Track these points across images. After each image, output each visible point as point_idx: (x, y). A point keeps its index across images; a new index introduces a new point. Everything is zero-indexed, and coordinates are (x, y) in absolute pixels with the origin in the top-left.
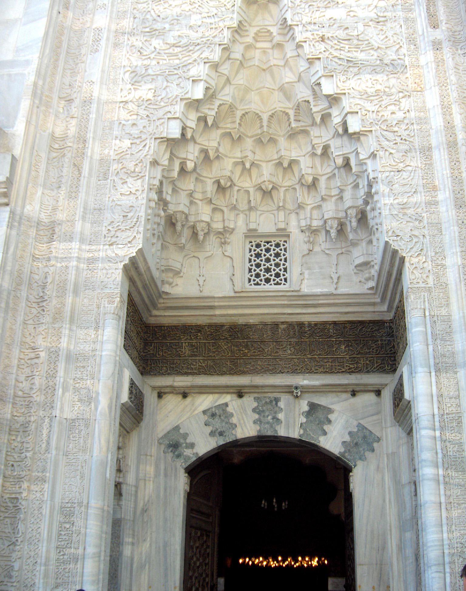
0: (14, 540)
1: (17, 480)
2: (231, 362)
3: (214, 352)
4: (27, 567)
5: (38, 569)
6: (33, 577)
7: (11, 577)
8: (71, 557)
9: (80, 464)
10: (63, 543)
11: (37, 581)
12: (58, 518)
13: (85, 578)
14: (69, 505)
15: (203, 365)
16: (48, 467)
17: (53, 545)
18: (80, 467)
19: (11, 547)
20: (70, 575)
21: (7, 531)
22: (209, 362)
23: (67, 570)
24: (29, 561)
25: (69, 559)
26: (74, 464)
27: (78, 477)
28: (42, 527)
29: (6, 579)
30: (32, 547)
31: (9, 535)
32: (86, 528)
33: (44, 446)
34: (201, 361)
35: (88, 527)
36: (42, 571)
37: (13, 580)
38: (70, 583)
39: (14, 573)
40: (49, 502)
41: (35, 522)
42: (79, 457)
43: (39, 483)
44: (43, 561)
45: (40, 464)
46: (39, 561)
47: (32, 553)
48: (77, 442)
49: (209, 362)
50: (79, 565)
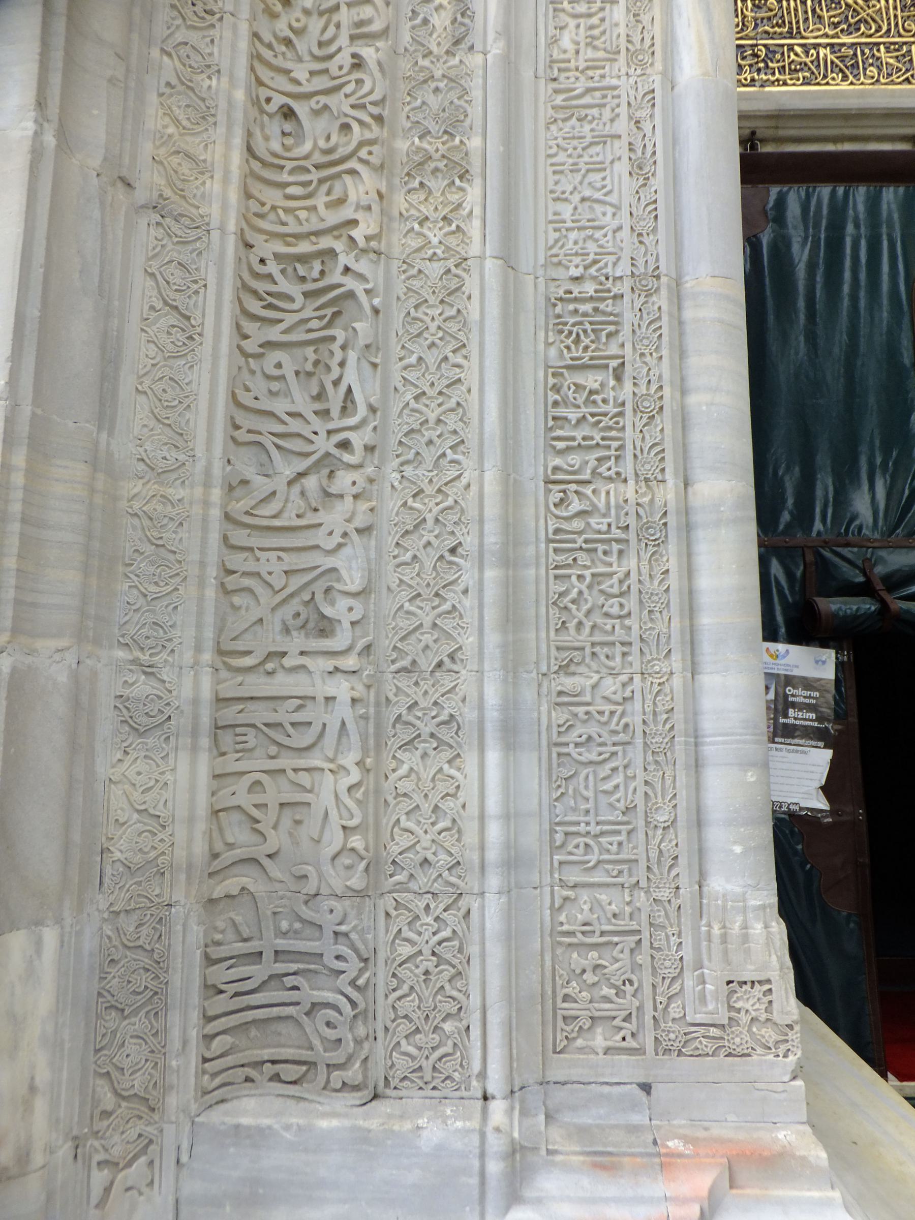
0: (324, 444)
1: (314, 176)
2: (888, 50)
3: (836, 25)
4: (408, 575)
5: (468, 578)
6: (447, 624)
7: (325, 627)
8: (632, 521)
9: (623, 110)
10: (575, 459)
11: (469, 641)
12: (540, 349)
13: (706, 620)
14: (589, 288)
15: (805, 59)
16: (475, 112)
17: (534, 466)
18: (622, 126)
19: (311, 483)
20: (631, 603)
21: (280, 407)
22: (822, 52)
23: (612, 585)
24: (415, 543)
25: (617, 533)
26: (595, 112)
27: (622, 168)
28: (471, 378)
29: (298, 641)
30: (420, 474)
31: (295, 426)
32: (684, 392)
33: (441, 21)
34: (798, 49)
35: (692, 382)
36: (491, 593)
37: (338, 642)
38: (635, 649)
39: (343, 603)
40: (491, 265)
41: (432, 358)
42: (614, 82)
43: (437, 184)
44: (492, 539)
45: (434, 101)
46: (470, 542)
47: (429, 507)
48: (595, 20)
49: (822, 52)
50: (672, 559)
